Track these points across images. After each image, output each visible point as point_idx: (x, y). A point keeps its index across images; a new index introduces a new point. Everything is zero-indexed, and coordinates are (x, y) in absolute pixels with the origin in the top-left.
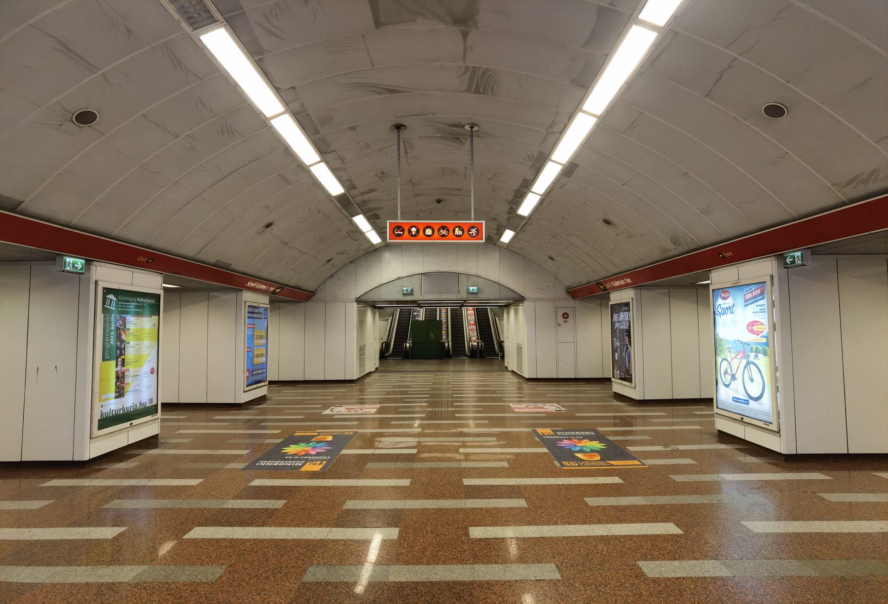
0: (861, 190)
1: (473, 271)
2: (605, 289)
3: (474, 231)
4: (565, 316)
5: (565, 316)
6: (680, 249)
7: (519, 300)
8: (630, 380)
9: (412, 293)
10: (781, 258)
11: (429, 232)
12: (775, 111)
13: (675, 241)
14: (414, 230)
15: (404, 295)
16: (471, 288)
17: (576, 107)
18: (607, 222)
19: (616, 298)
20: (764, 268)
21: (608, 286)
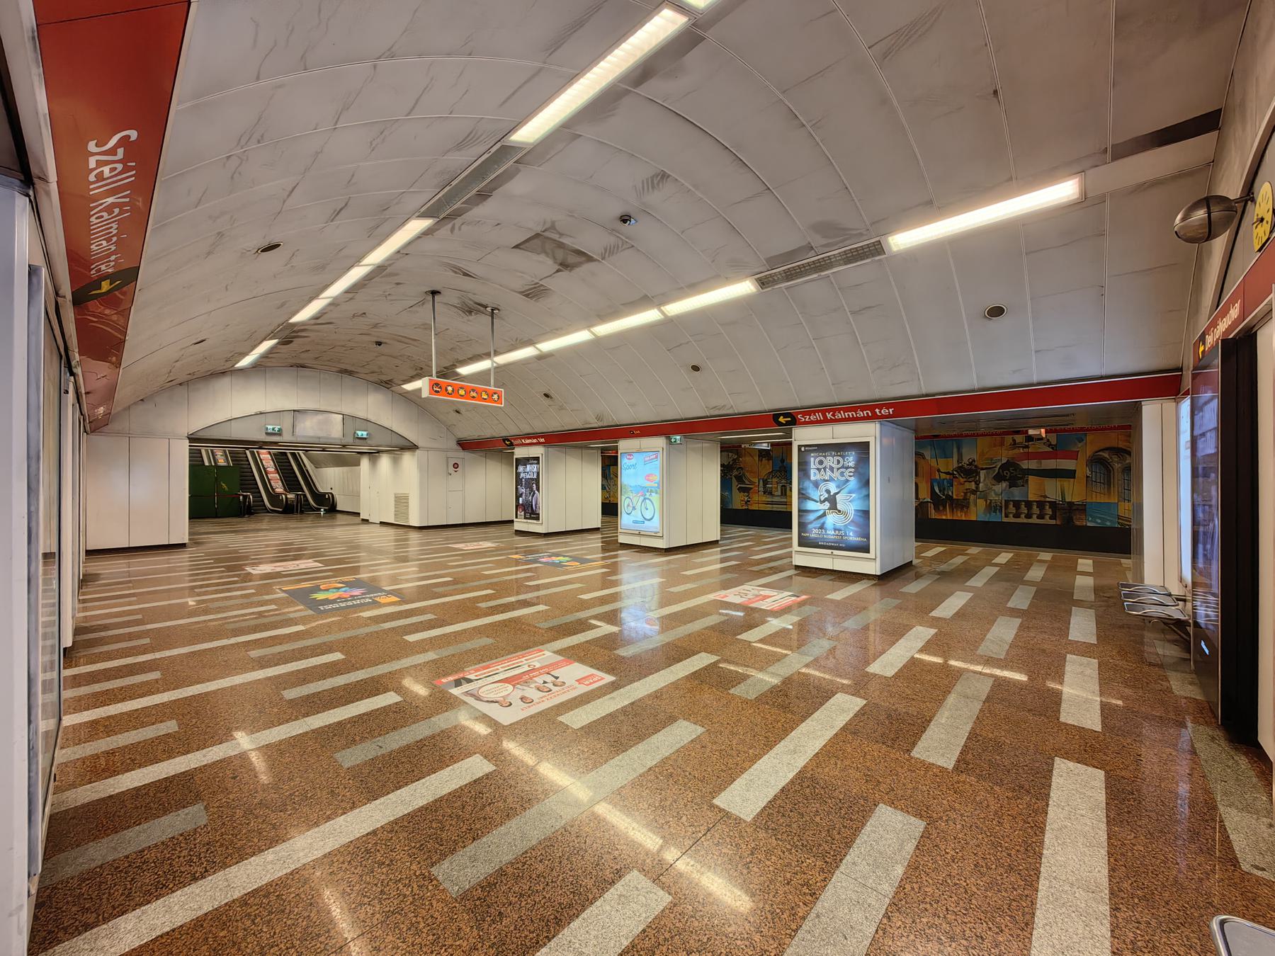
0: (717, 413)
1: (362, 415)
2: (512, 444)
3: (495, 397)
4: (456, 466)
5: (456, 466)
6: (600, 424)
7: (413, 447)
8: (538, 519)
9: (280, 433)
10: (669, 439)
11: (462, 392)
12: (696, 368)
13: (599, 418)
14: (450, 388)
15: (267, 434)
16: (360, 433)
17: (589, 327)
18: (547, 395)
19: (520, 452)
20: (659, 442)
21: (515, 442)
